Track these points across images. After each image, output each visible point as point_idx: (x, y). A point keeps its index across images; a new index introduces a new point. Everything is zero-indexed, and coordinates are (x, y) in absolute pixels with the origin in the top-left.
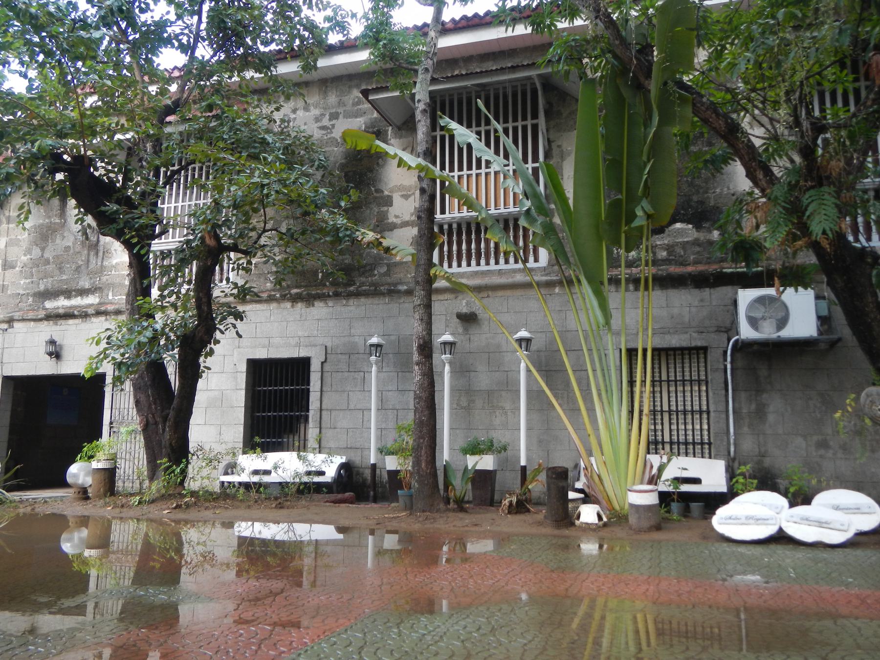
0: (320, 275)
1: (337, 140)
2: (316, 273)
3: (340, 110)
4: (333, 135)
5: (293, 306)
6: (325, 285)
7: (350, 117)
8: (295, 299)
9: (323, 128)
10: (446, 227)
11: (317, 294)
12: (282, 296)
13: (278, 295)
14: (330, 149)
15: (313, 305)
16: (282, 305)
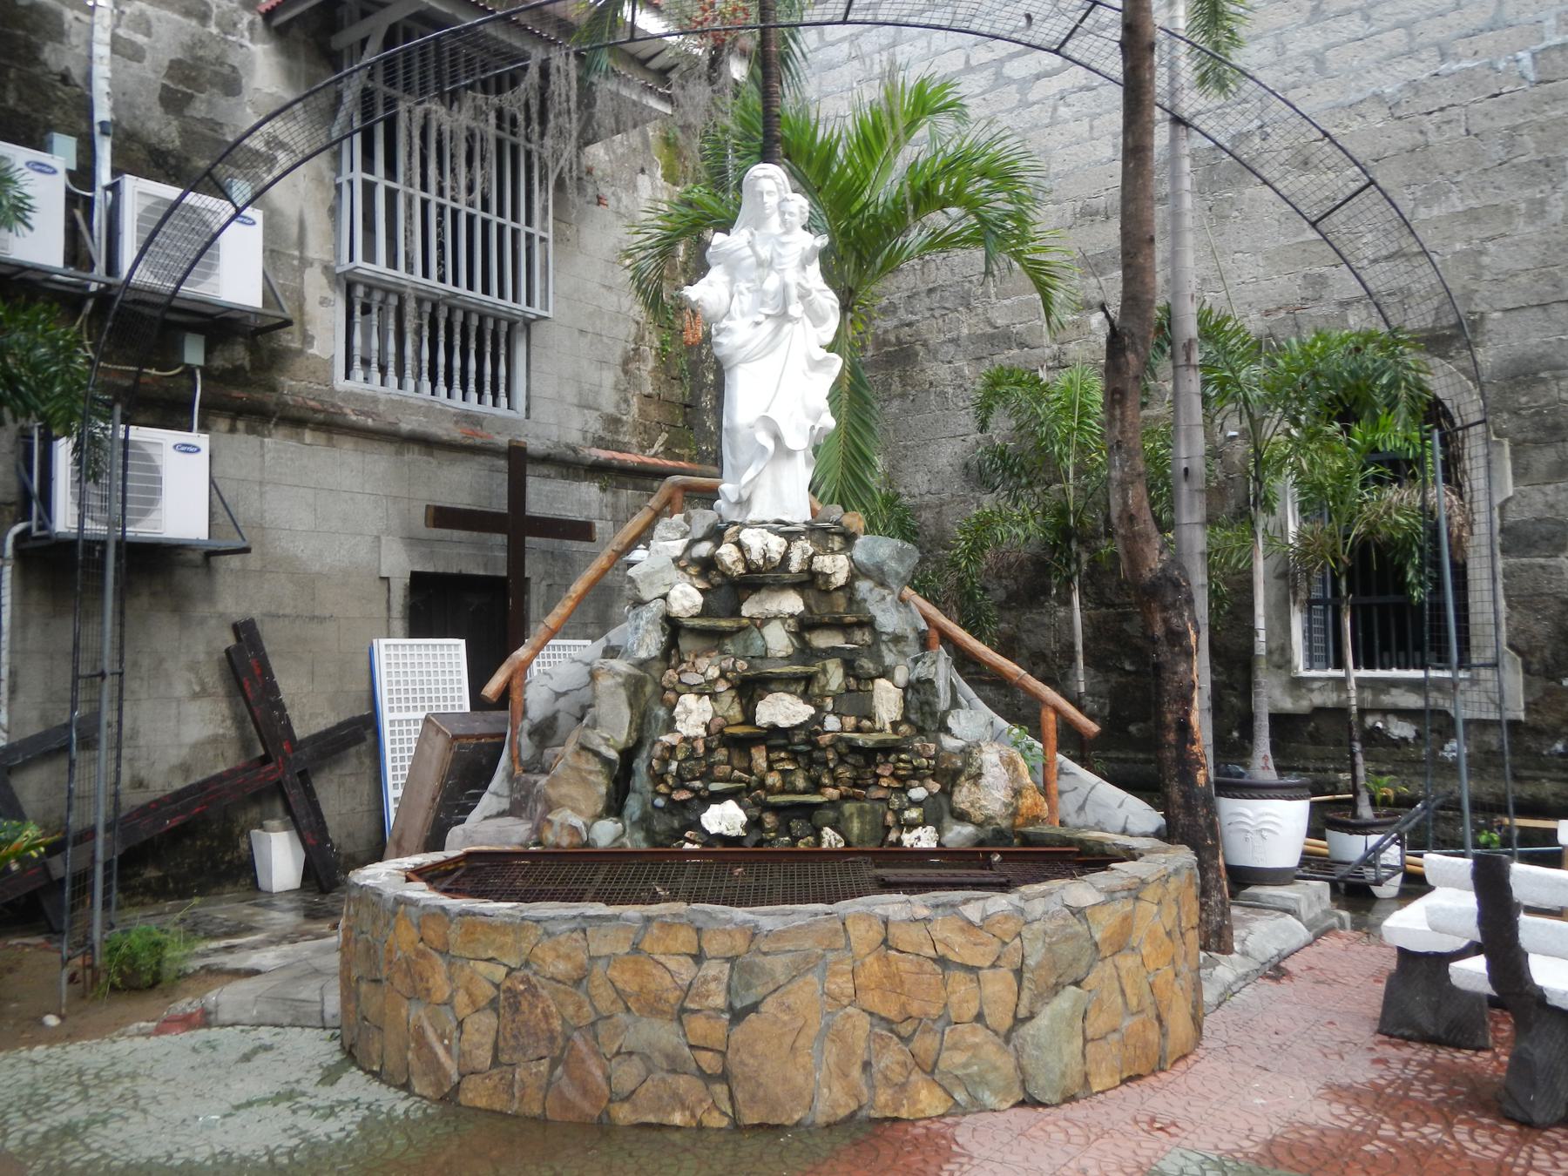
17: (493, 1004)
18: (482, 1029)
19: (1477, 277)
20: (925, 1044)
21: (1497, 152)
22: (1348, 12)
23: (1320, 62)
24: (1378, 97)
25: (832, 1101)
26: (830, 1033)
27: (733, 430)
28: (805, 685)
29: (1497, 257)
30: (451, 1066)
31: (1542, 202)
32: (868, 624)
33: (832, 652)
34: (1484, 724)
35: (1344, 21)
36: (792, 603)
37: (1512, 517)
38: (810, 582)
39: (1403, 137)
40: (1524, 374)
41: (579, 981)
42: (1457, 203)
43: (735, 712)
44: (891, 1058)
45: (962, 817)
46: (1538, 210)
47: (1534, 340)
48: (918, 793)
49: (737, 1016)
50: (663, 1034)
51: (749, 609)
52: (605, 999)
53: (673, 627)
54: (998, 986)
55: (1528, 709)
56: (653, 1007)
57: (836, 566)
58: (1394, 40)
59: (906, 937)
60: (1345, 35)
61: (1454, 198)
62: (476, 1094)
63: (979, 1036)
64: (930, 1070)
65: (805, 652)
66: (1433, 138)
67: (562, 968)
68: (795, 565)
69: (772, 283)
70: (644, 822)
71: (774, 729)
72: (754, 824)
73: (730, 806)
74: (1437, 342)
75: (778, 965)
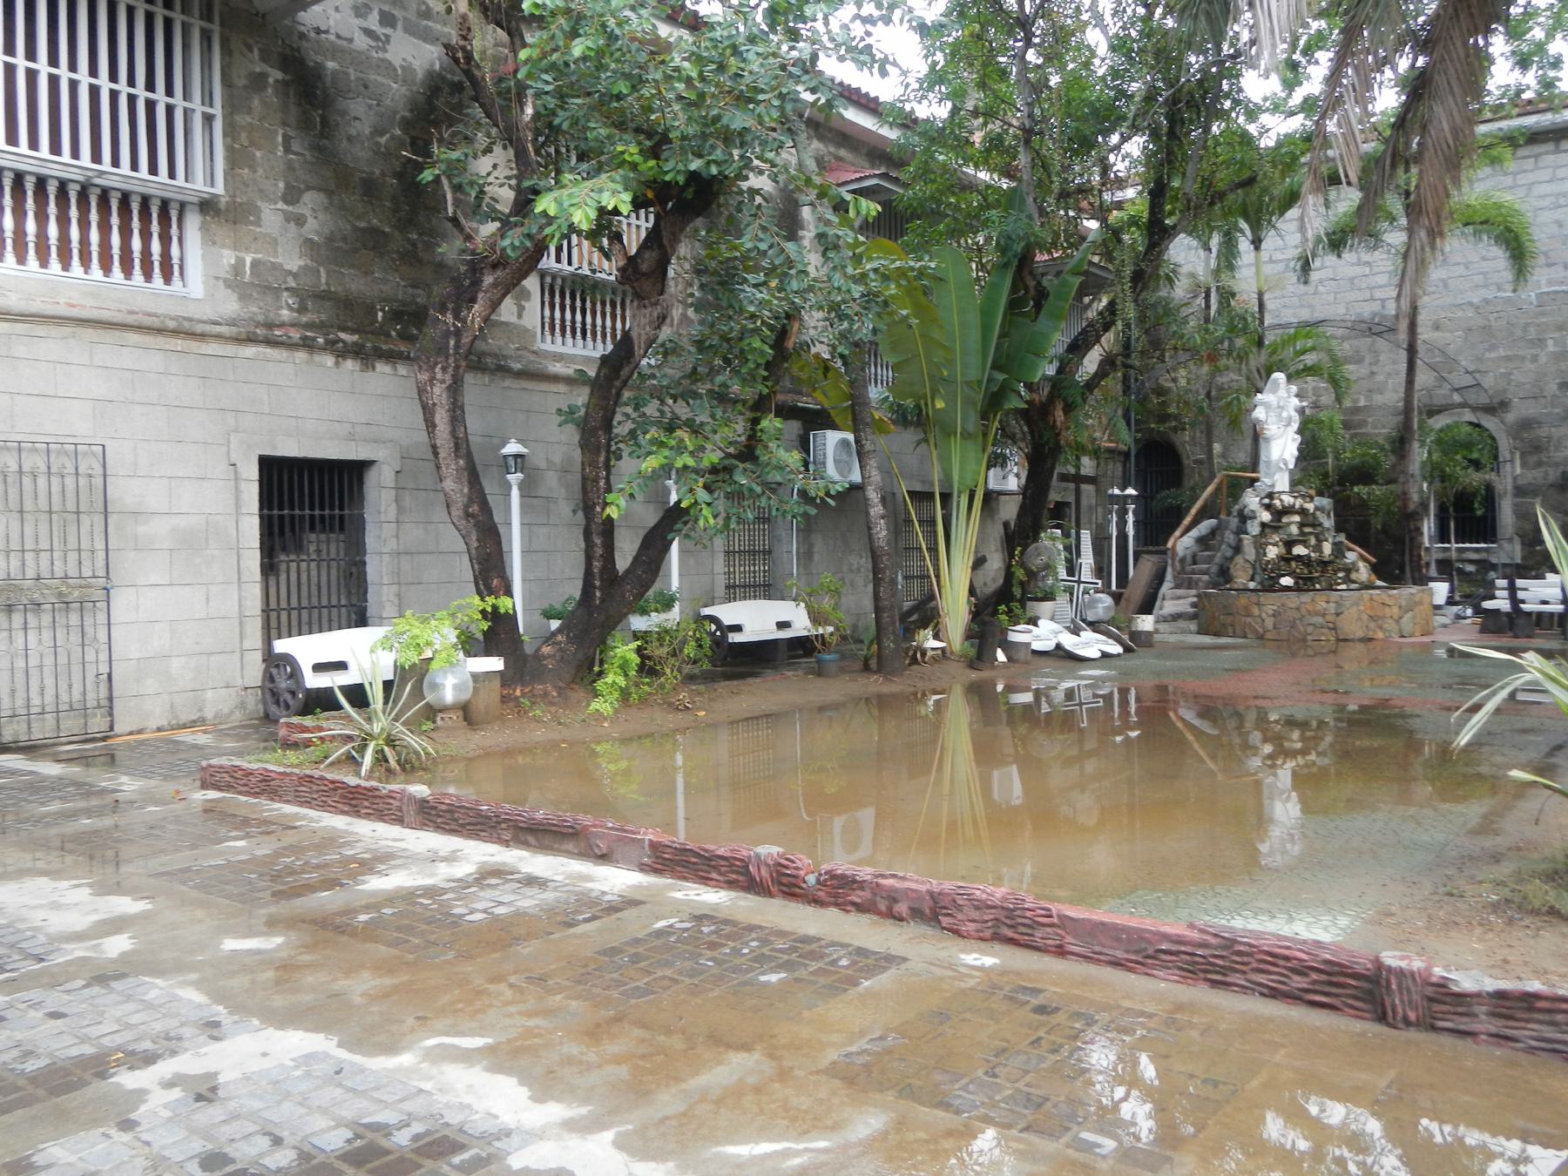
0: (380, 314)
1: (395, 70)
2: (371, 311)
3: (397, 13)
4: (388, 56)
5: (337, 364)
6: (389, 336)
7: (413, 34)
8: (343, 352)
9: (369, 33)
10: (548, 280)
11: (391, 351)
12: (327, 342)
13: (321, 340)
14: (384, 81)
15: (374, 368)
16: (317, 358)
17: (1274, 615)
18: (1269, 623)
19: (1509, 384)
20: (1380, 622)
21: (1519, 332)
22: (1459, 264)
23: (1446, 285)
24: (1470, 304)
25: (1360, 634)
26: (1359, 619)
27: (1268, 463)
28: (1305, 543)
29: (1517, 376)
30: (1261, 631)
31: (1537, 355)
32: (1320, 525)
33: (1311, 533)
34: (1505, 565)
35: (1456, 268)
36: (1297, 518)
37: (1520, 482)
38: (1303, 512)
39: (1481, 322)
40: (1526, 425)
41: (1298, 609)
42: (1502, 352)
43: (1284, 551)
44: (1372, 625)
45: (1354, 582)
46: (1535, 358)
47: (1531, 411)
48: (1340, 575)
49: (1338, 615)
50: (1320, 620)
51: (1285, 520)
52: (1304, 612)
53: (1263, 525)
54: (1395, 610)
55: (1523, 558)
56: (1317, 614)
57: (1310, 507)
58: (1478, 279)
59: (1375, 598)
60: (1456, 274)
61: (1501, 350)
62: (1268, 636)
63: (1391, 621)
64: (1380, 628)
65: (1302, 533)
66: (1493, 324)
67: (1293, 605)
68: (1297, 506)
69: (1285, 414)
70: (1261, 583)
71: (1299, 556)
72: (1296, 583)
73: (1287, 578)
74: (1490, 410)
75: (1347, 603)
